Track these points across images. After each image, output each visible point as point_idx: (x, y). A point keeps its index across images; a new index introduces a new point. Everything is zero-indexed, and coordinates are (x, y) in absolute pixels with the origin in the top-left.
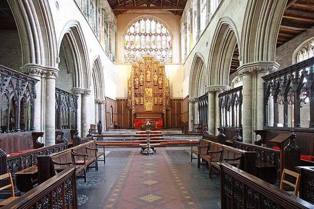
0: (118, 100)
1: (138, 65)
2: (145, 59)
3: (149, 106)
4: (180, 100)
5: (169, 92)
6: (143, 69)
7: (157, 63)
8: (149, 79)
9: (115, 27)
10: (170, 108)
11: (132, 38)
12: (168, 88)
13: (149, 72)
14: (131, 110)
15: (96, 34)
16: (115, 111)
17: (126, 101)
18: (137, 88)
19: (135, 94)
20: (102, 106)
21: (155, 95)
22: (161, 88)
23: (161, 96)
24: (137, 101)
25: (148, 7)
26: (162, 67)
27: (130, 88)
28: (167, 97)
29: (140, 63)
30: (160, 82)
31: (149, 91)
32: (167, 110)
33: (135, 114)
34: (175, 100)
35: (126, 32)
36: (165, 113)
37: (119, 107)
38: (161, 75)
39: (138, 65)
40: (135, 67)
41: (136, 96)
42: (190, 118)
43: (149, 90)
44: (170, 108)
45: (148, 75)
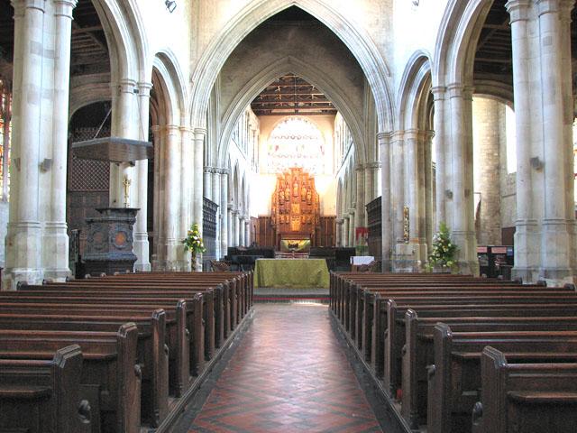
0: (260, 218)
1: (284, 177)
2: (292, 170)
3: (295, 225)
4: (331, 219)
5: (319, 209)
6: (290, 182)
7: (306, 174)
8: (296, 194)
9: (258, 131)
10: (319, 228)
11: (277, 142)
12: (318, 204)
13: (296, 185)
14: (275, 230)
15: (237, 142)
16: (258, 232)
17: (270, 219)
18: (282, 204)
19: (280, 211)
20: (248, 226)
21: (303, 212)
22: (310, 204)
23: (310, 213)
24: (283, 219)
25: (296, 113)
26: (312, 179)
27: (274, 205)
28: (316, 215)
29: (287, 175)
30: (309, 197)
31: (296, 208)
32: (316, 230)
33: (279, 235)
34: (325, 218)
35: (269, 134)
36: (314, 233)
37: (262, 226)
38: (311, 188)
39: (284, 177)
40: (280, 179)
41: (281, 213)
42: (338, 240)
43: (296, 205)
44: (319, 228)
45: (296, 189)
